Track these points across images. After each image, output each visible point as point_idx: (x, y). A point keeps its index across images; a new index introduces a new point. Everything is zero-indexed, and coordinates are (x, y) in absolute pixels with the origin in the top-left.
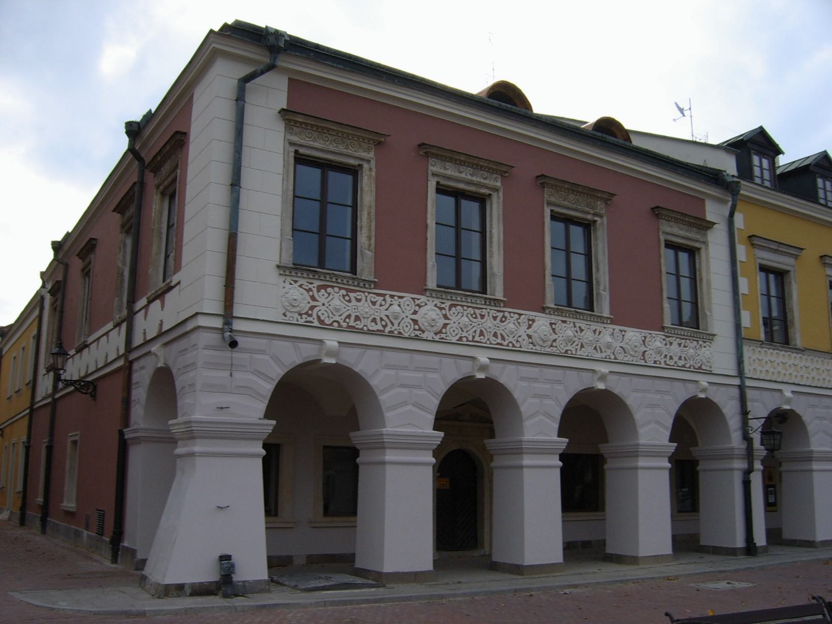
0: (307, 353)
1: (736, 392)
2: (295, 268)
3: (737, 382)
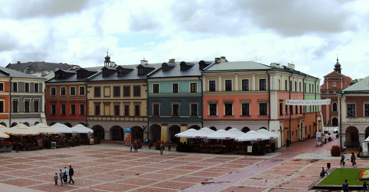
0: (350, 126)
2: (347, 117)
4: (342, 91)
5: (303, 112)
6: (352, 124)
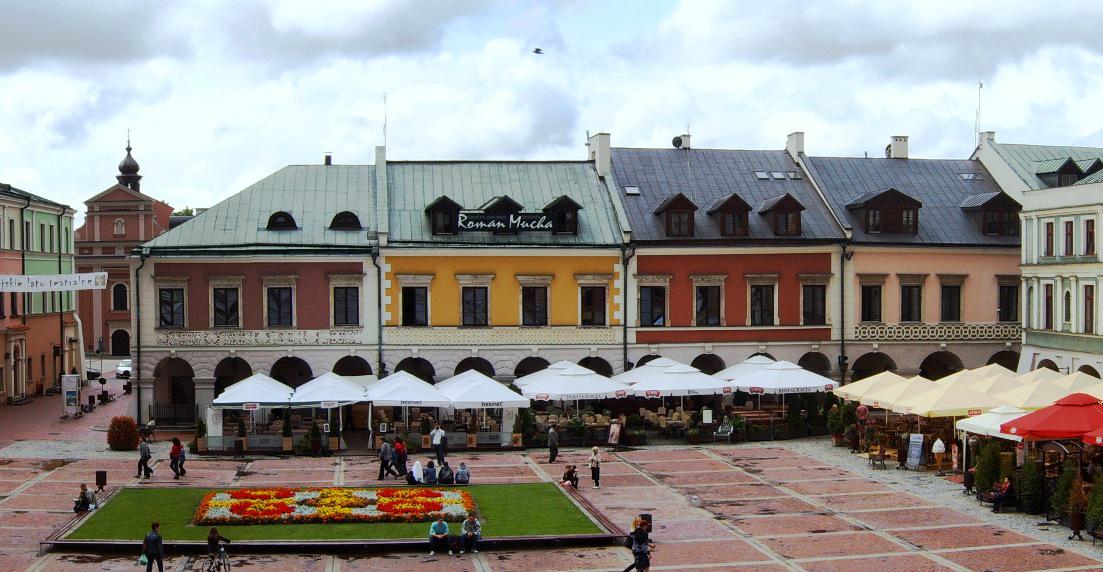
0: (166, 355)
1: (377, 352)
2: (159, 328)
3: (383, 347)
4: (142, 248)
5: (20, 313)
6: (173, 351)
